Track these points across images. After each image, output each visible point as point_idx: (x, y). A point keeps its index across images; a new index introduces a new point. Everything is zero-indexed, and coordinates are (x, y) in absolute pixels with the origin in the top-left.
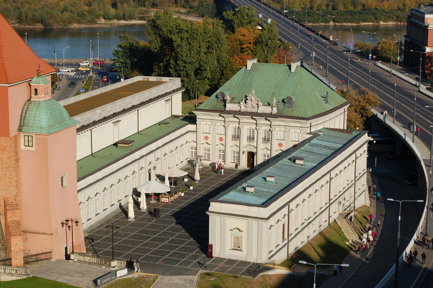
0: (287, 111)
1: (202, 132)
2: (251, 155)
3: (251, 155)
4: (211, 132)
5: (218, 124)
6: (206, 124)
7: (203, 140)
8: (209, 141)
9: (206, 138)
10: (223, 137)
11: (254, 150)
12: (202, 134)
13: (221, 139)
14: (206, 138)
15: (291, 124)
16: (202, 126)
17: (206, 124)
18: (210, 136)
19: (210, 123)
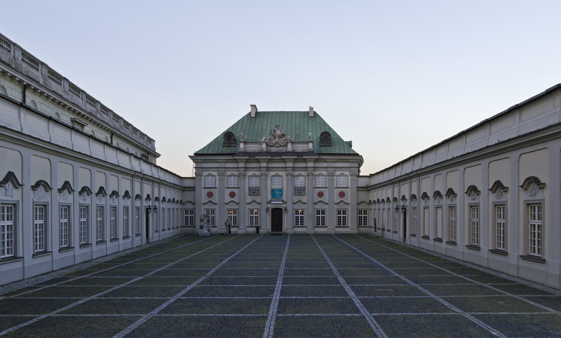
0: (324, 150)
1: (203, 186)
2: (277, 215)
3: (277, 215)
4: (217, 186)
5: (229, 173)
6: (208, 175)
7: (204, 198)
8: (216, 198)
9: (210, 195)
10: (235, 191)
11: (283, 206)
12: (203, 190)
13: (232, 195)
14: (210, 195)
15: (337, 165)
16: (203, 178)
17: (208, 175)
18: (216, 192)
19: (215, 173)
